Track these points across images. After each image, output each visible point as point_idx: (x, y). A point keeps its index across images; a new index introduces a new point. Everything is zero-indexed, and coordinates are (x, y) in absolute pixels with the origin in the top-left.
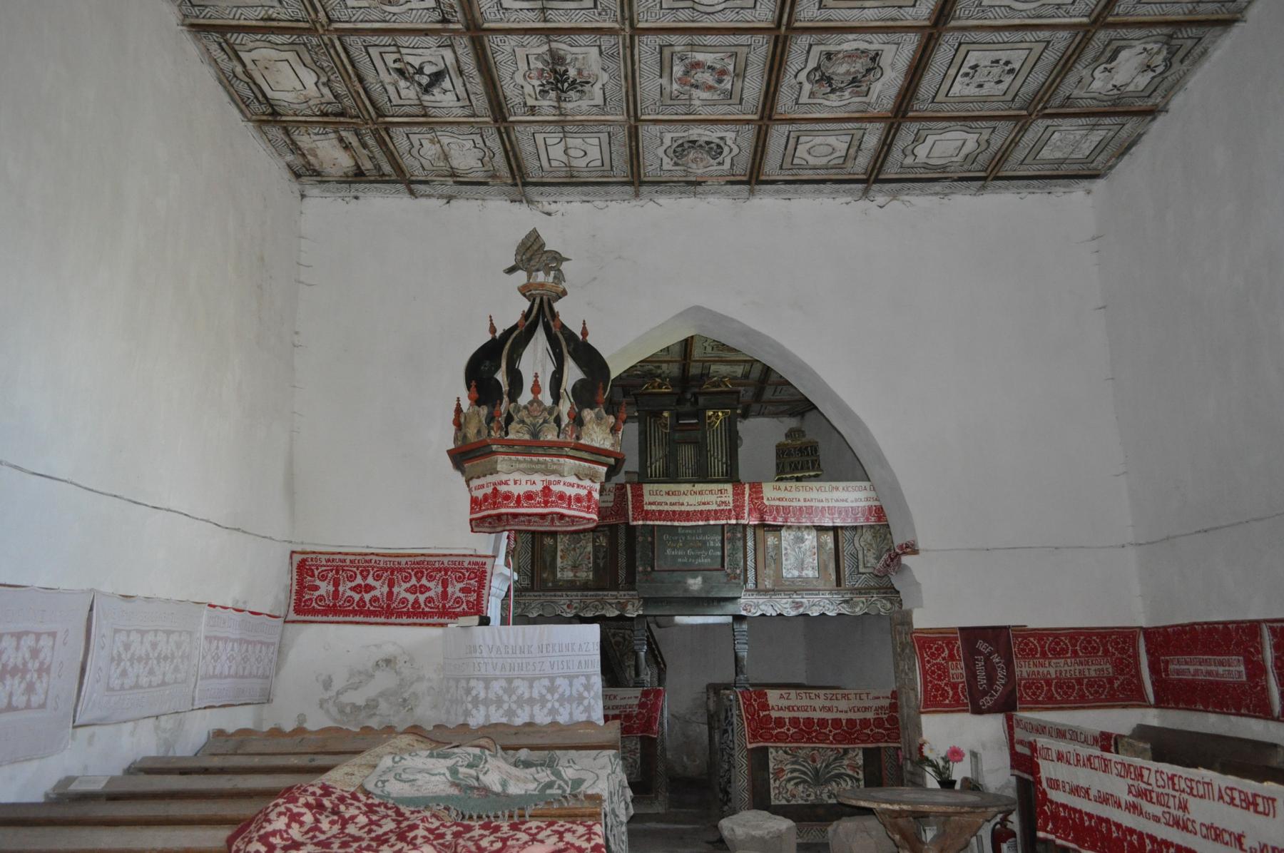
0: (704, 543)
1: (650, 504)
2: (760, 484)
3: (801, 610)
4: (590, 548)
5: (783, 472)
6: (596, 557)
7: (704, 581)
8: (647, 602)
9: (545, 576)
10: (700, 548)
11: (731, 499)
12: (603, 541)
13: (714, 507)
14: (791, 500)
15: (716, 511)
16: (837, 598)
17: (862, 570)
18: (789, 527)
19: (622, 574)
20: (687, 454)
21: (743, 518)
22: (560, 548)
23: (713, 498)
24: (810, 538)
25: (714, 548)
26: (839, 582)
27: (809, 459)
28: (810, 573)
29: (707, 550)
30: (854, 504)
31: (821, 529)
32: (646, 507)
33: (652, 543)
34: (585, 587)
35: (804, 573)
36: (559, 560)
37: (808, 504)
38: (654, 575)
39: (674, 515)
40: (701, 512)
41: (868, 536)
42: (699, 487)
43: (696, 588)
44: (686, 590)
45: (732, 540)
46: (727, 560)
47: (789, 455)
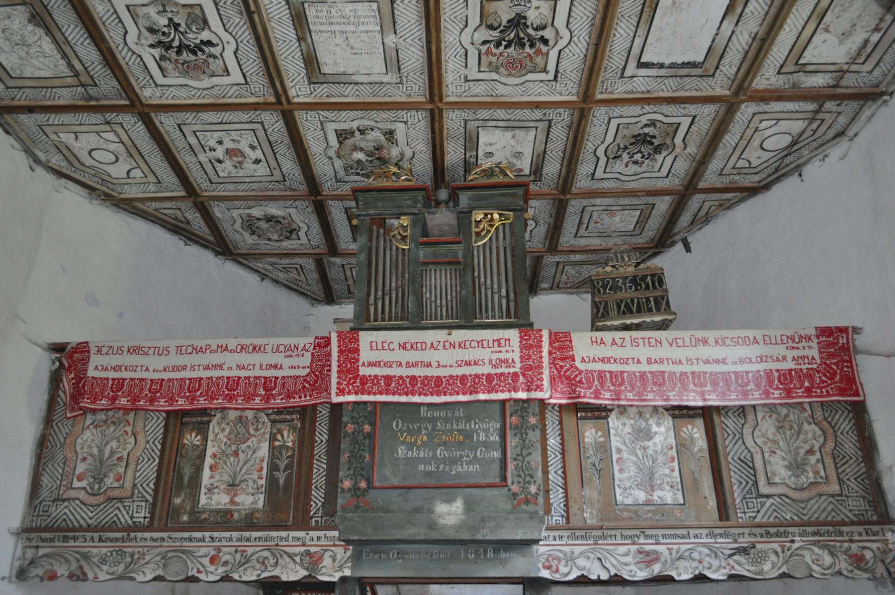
0: (468, 435)
1: (370, 364)
2: (567, 335)
3: (657, 569)
4: (264, 450)
5: (606, 316)
6: (273, 467)
7: (469, 507)
8: (361, 548)
9: (178, 501)
10: (460, 445)
11: (516, 356)
12: (289, 438)
13: (486, 369)
14: (625, 361)
15: (489, 377)
16: (725, 544)
17: (764, 489)
18: (623, 410)
19: (317, 497)
20: (439, 284)
21: (539, 388)
22: (209, 453)
23: (485, 354)
24: (663, 432)
25: (487, 445)
26: (723, 510)
27: (651, 294)
28: (668, 496)
29: (474, 447)
30: (740, 368)
31: (681, 413)
32: (363, 371)
33: (371, 436)
34: (250, 523)
35: (656, 496)
36: (206, 472)
37: (655, 368)
38: (372, 495)
39: (412, 384)
40: (463, 378)
41: (768, 426)
42: (459, 335)
43: (451, 521)
44: (432, 526)
45: (521, 429)
46: (511, 466)
47: (615, 288)
